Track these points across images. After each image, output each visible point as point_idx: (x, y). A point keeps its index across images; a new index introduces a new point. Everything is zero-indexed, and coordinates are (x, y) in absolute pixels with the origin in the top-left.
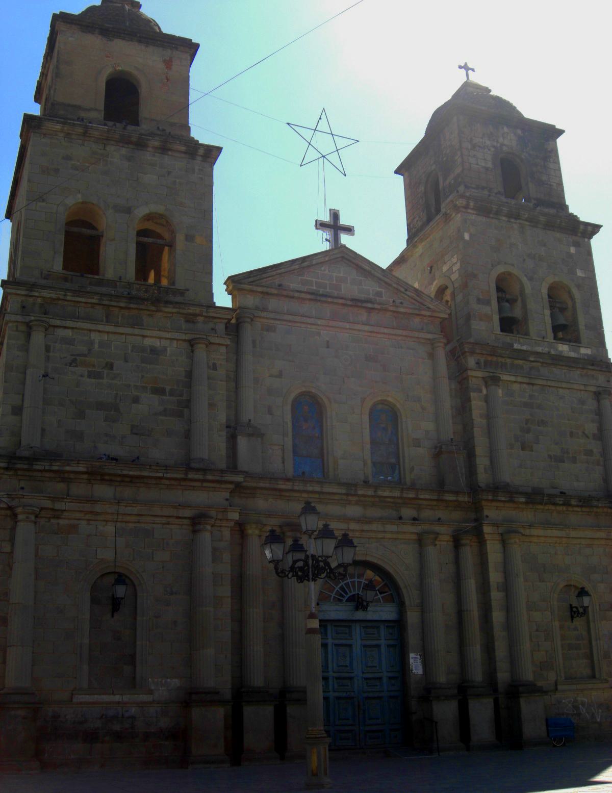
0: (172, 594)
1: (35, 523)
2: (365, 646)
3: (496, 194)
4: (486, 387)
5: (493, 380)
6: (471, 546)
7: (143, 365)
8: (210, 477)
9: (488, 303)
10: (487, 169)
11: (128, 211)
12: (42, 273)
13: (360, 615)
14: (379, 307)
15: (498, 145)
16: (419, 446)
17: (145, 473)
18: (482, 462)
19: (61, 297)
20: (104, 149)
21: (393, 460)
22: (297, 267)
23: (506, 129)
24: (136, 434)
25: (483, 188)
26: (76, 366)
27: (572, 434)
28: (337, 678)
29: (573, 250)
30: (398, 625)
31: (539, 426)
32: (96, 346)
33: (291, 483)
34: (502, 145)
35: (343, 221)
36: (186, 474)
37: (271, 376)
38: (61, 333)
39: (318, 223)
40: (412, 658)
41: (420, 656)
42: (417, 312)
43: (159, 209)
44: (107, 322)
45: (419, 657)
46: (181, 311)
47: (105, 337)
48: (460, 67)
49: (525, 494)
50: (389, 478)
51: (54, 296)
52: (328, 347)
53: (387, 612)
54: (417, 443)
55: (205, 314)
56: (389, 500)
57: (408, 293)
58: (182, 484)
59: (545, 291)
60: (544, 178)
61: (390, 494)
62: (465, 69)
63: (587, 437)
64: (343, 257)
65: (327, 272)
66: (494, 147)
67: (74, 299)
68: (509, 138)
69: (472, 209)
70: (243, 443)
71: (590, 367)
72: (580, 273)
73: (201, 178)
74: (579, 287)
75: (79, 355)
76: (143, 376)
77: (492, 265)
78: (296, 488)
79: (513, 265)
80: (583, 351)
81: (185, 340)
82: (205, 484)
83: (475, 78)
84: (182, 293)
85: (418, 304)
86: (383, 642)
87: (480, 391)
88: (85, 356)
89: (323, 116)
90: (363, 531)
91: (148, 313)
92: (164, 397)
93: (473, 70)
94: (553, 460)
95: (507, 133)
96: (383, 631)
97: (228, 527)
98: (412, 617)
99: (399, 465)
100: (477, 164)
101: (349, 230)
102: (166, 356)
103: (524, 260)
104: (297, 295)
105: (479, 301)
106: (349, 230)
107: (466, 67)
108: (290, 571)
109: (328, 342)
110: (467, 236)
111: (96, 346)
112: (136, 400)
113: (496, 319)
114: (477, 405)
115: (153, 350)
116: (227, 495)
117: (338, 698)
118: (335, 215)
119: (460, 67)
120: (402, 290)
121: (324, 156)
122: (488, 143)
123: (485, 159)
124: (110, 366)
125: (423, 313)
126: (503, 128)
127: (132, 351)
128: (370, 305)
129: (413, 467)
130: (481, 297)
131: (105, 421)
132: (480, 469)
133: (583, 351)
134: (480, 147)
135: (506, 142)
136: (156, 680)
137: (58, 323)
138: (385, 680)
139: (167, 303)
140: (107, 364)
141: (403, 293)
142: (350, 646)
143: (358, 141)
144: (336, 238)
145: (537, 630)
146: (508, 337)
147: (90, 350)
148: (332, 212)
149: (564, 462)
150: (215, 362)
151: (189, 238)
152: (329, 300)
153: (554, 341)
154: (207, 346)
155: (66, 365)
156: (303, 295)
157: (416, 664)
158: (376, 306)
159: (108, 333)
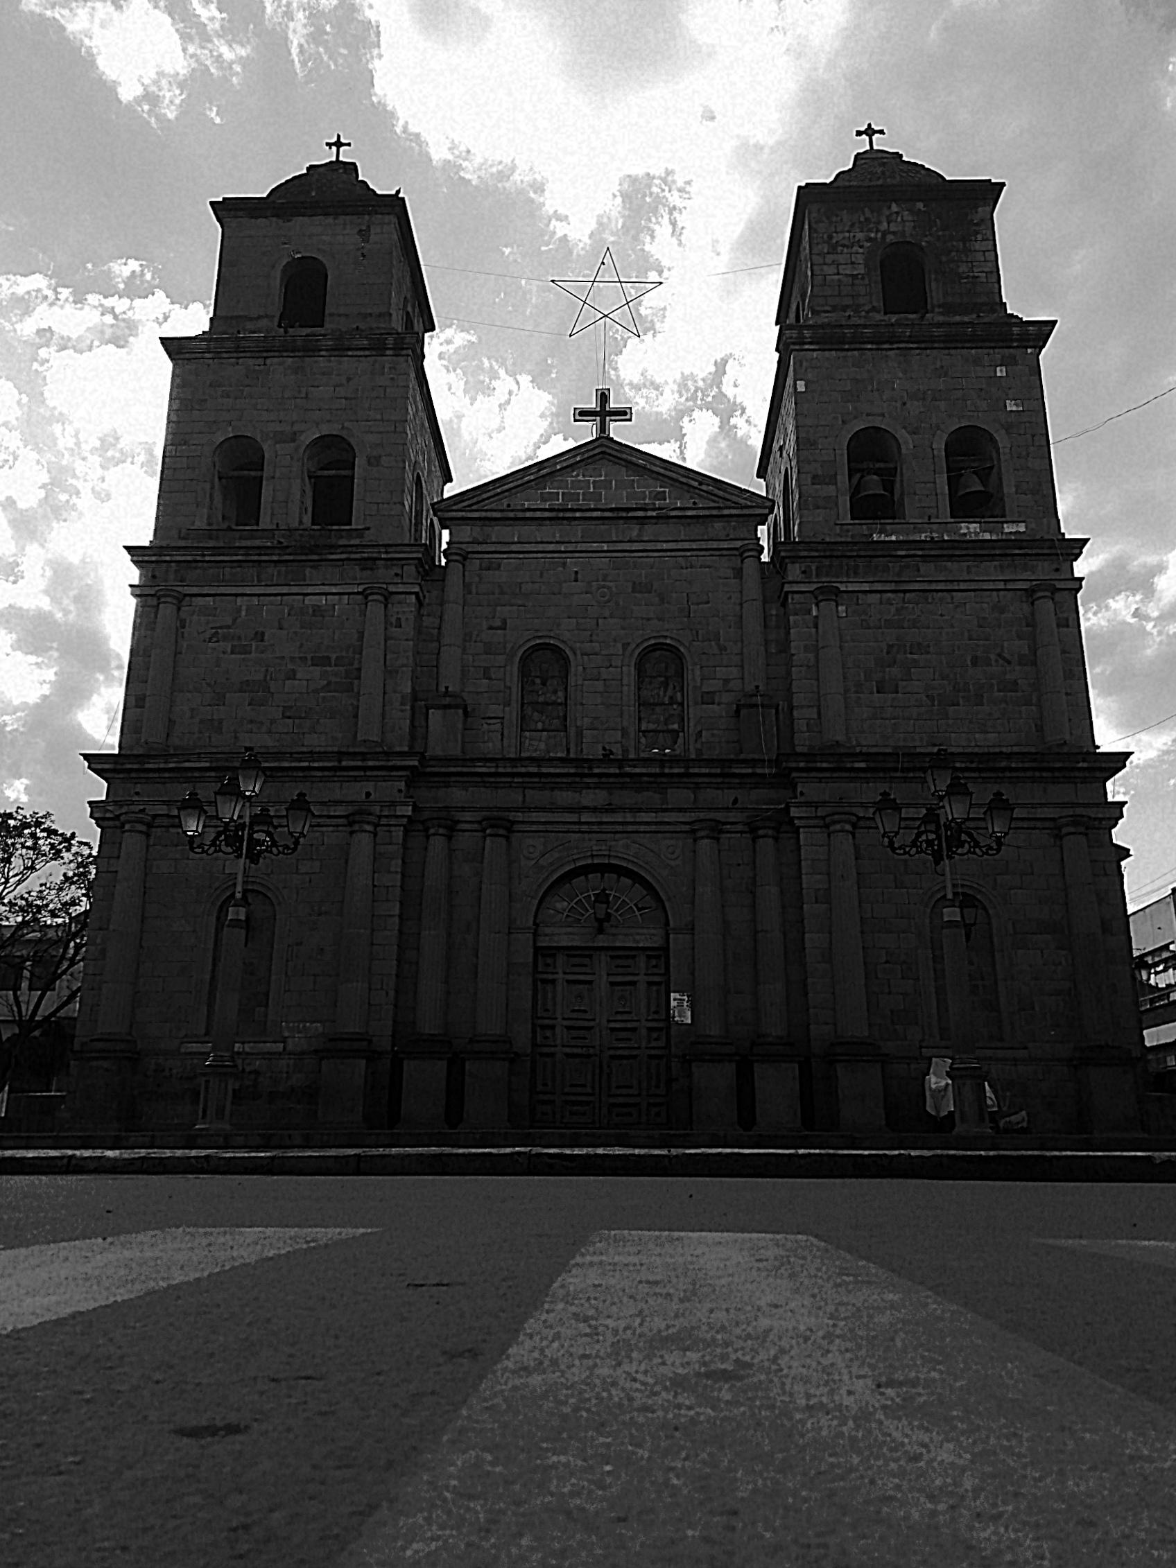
0: (320, 915)
1: (148, 835)
2: (612, 984)
3: (867, 312)
4: (817, 605)
5: (831, 594)
6: (776, 839)
7: (303, 630)
8: (370, 763)
9: (833, 480)
10: (854, 276)
11: (293, 438)
12: (180, 532)
13: (601, 941)
14: (654, 514)
15: (879, 235)
16: (713, 703)
17: (286, 764)
18: (803, 716)
19: (199, 558)
20: (265, 364)
21: (676, 726)
22: (532, 477)
23: (894, 208)
24: (289, 718)
25: (845, 308)
26: (217, 642)
27: (975, 662)
28: (569, 1028)
29: (1001, 372)
30: (662, 953)
31: (911, 653)
32: (243, 613)
33: (494, 764)
34: (884, 234)
35: (613, 404)
36: (340, 761)
37: (491, 628)
38: (200, 601)
39: (577, 411)
40: (675, 1000)
41: (688, 996)
42: (715, 512)
43: (334, 429)
44: (258, 581)
45: (686, 998)
46: (353, 556)
47: (255, 600)
48: (859, 133)
49: (866, 756)
50: (667, 751)
51: (189, 558)
52: (576, 580)
53: (648, 937)
54: (708, 698)
55: (383, 556)
56: (645, 779)
57: (704, 487)
58: (338, 774)
59: (940, 445)
60: (963, 268)
61: (644, 771)
62: (867, 135)
63: (1009, 662)
64: (602, 453)
65: (580, 478)
66: (869, 240)
67: (213, 558)
68: (899, 219)
69: (810, 343)
70: (435, 716)
71: (1017, 552)
72: (1011, 406)
73: (392, 379)
74: (1008, 428)
75: (221, 628)
76: (301, 645)
77: (843, 421)
78: (501, 770)
79: (883, 415)
80: (1008, 528)
81: (358, 593)
82: (368, 773)
83: (879, 143)
84: (360, 533)
85: (721, 501)
86: (641, 978)
87: (809, 611)
88: (228, 627)
89: (607, 260)
90: (601, 823)
91: (312, 564)
92: (328, 669)
93: (881, 132)
94: (936, 703)
95: (897, 213)
96: (642, 961)
97: (400, 826)
98: (678, 942)
99: (683, 731)
100: (838, 274)
101: (624, 414)
102: (333, 616)
103: (904, 404)
104: (528, 514)
105: (816, 479)
106: (624, 414)
107: (870, 132)
108: (210, 846)
109: (576, 573)
110: (801, 386)
111: (243, 613)
112: (292, 675)
113: (845, 502)
114: (799, 633)
115: (317, 610)
116: (402, 785)
117: (568, 1055)
118: (604, 397)
119: (859, 133)
120: (696, 484)
121: (606, 316)
122: (860, 236)
123: (853, 263)
124: (260, 636)
125: (726, 512)
126: (889, 207)
127: (289, 615)
128: (640, 514)
129: (700, 732)
130: (820, 473)
131: (250, 704)
132: (801, 725)
133: (1008, 528)
134: (844, 246)
135: (893, 228)
136: (291, 1025)
137: (195, 590)
138: (644, 1032)
139: (333, 548)
140: (257, 633)
141: (696, 488)
142: (590, 982)
143: (661, 283)
144: (603, 428)
145: (887, 962)
146: (864, 527)
147: (235, 620)
148: (599, 393)
149: (958, 705)
150: (400, 616)
151: (373, 461)
152: (578, 515)
153: (952, 520)
154: (386, 599)
155: (205, 641)
156: (538, 514)
157: (680, 1007)
158: (650, 513)
159: (259, 595)
